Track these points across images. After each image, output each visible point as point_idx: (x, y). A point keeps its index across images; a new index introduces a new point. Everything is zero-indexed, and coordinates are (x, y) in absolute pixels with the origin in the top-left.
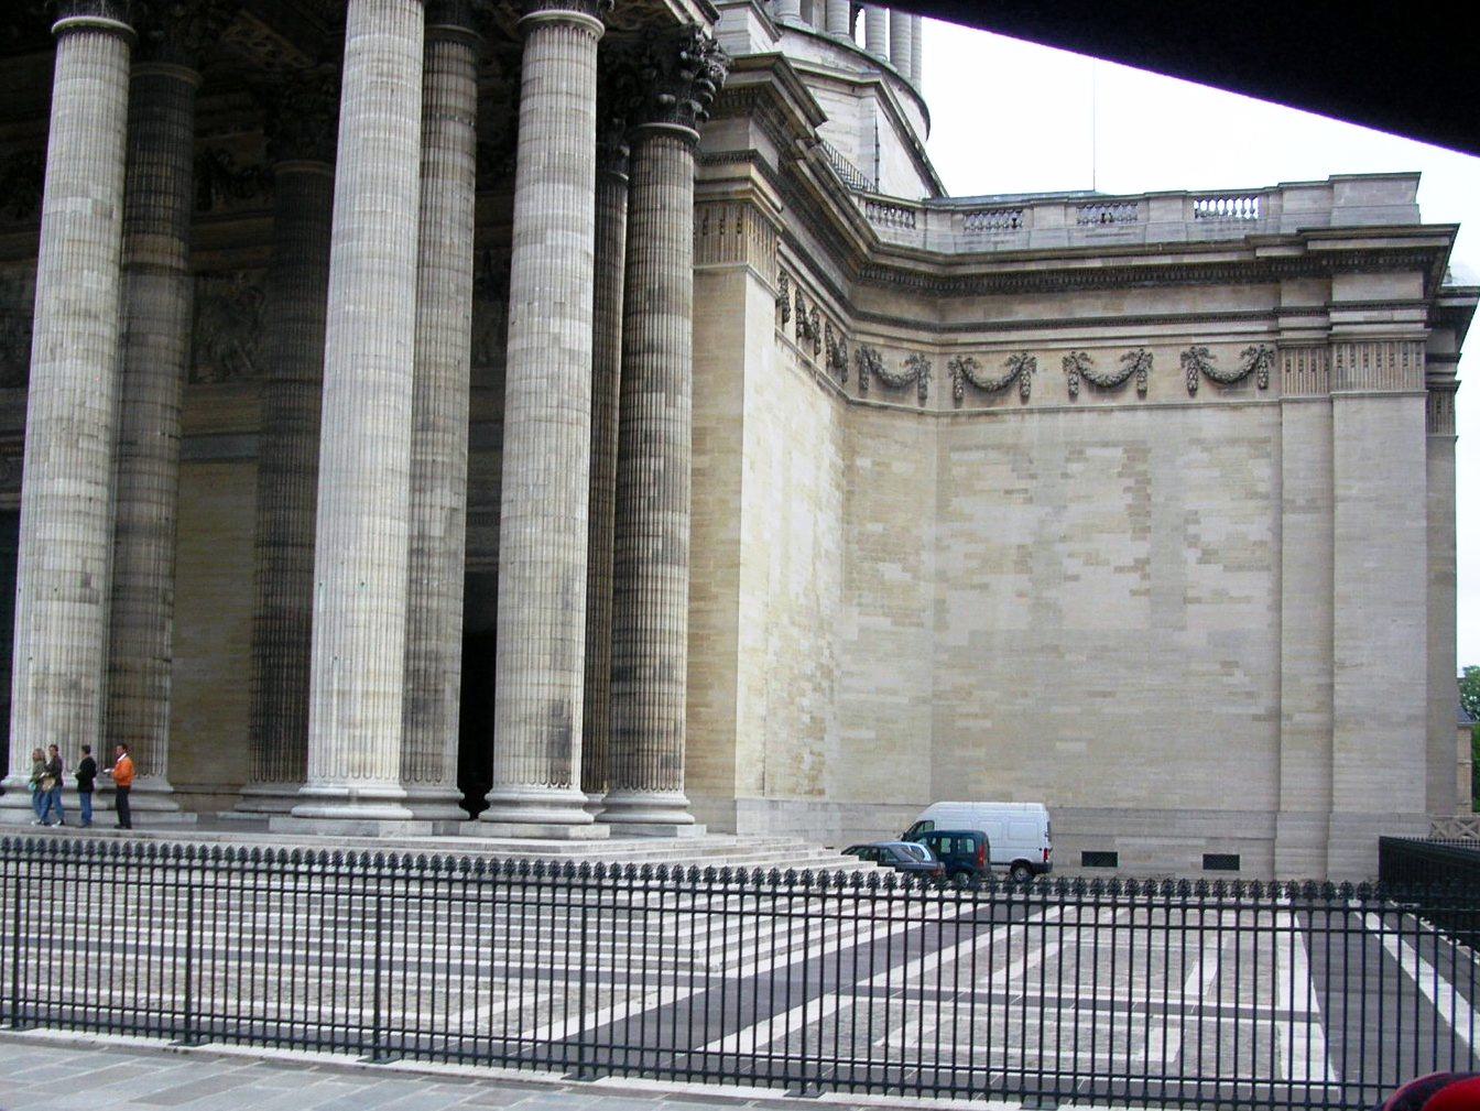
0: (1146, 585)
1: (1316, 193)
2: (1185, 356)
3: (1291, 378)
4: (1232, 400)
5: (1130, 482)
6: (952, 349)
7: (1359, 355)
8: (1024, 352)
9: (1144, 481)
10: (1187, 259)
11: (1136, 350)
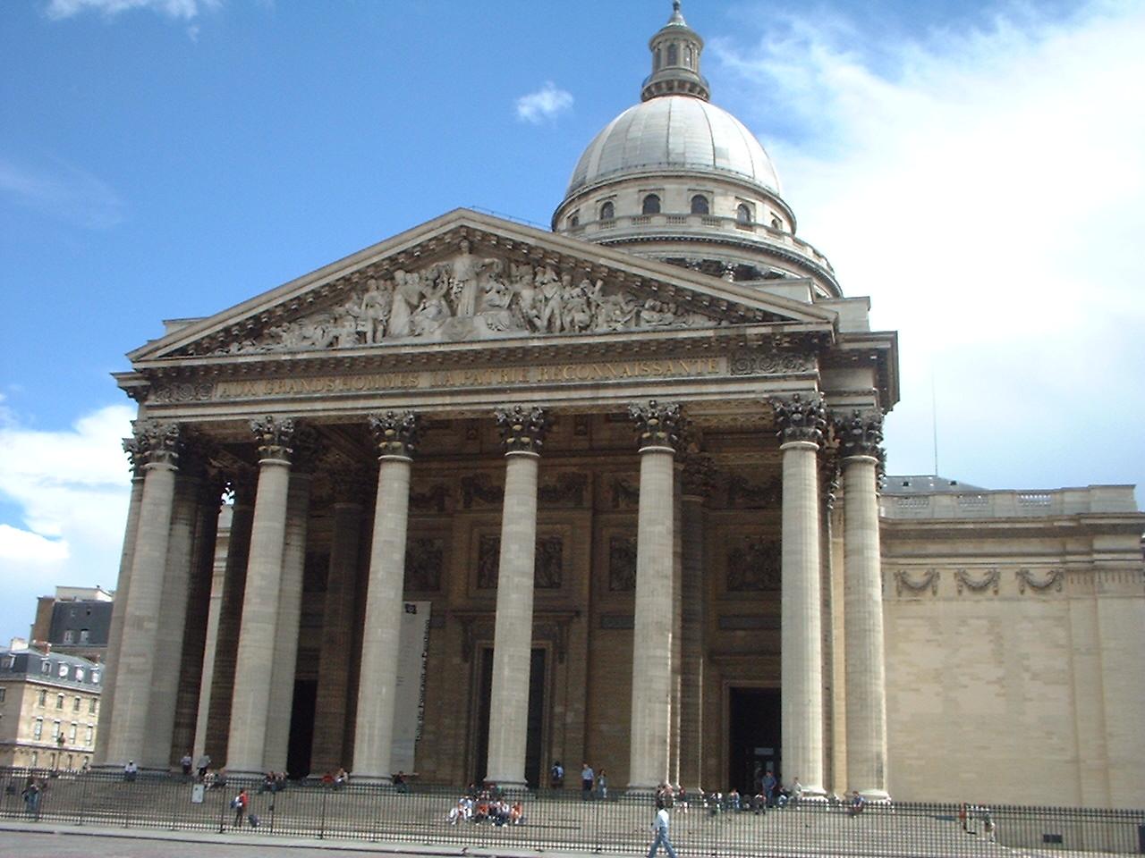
0: (1003, 691)
1: (1081, 494)
2: (1017, 574)
3: (1071, 586)
4: (1044, 597)
5: (992, 638)
6: (895, 567)
7: (1110, 576)
8: (934, 569)
10: (1018, 526)
11: (992, 570)
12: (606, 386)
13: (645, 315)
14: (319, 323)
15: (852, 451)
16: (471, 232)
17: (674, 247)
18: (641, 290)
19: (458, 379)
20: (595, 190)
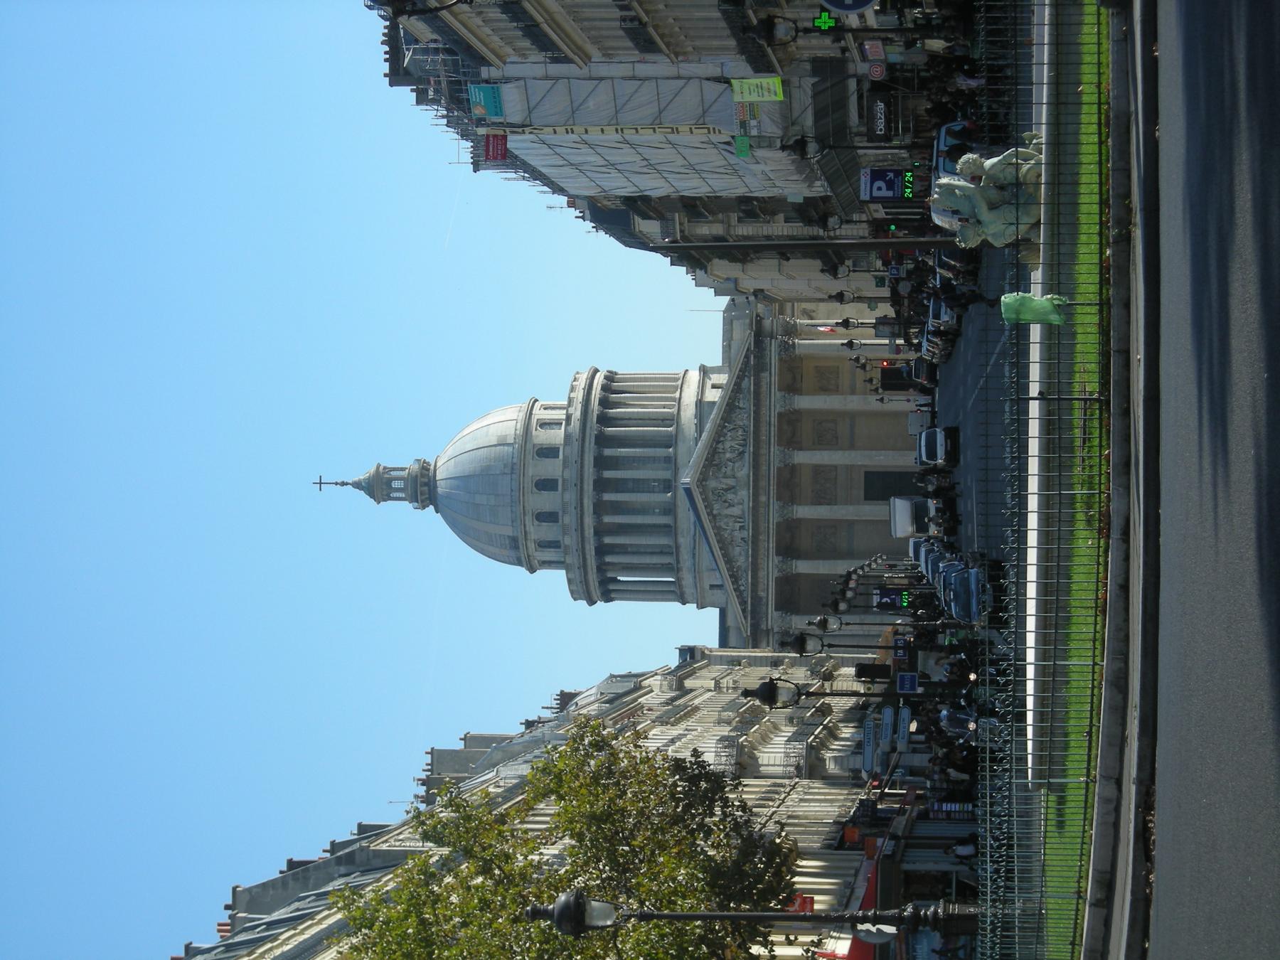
17: (586, 463)
19: (763, 483)
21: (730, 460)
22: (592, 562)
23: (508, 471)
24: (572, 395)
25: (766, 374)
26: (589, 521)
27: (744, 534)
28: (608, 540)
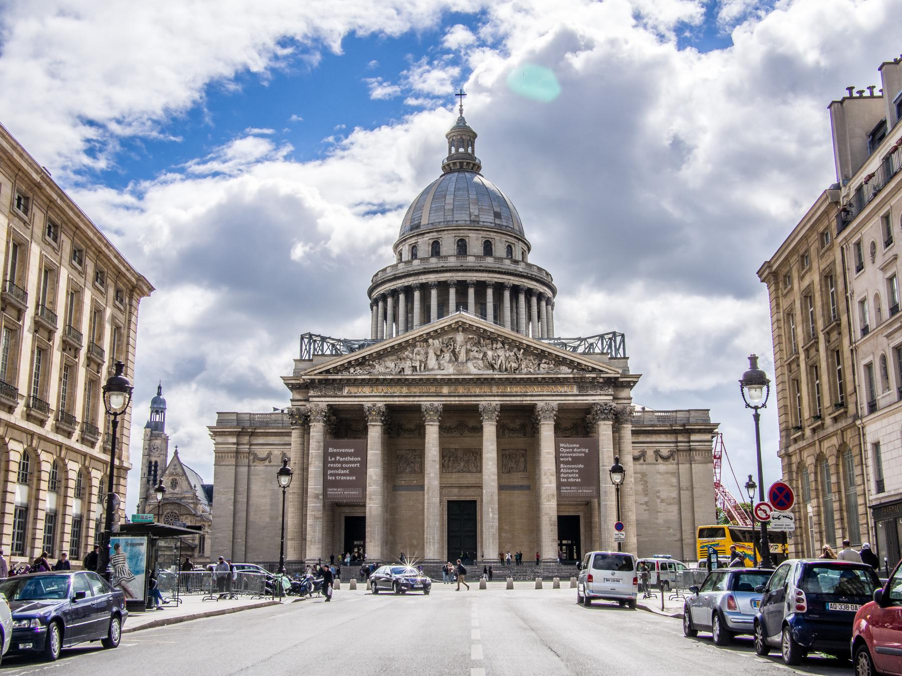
9: (646, 482)
12: (526, 396)
13: (542, 365)
14: (393, 361)
15: (622, 423)
16: (464, 323)
17: (480, 274)
18: (541, 355)
19: (461, 390)
20: (429, 233)
21: (485, 354)
22: (399, 284)
23: (473, 217)
24: (535, 269)
25: (575, 392)
26: (432, 278)
27: (408, 371)
28: (417, 295)
